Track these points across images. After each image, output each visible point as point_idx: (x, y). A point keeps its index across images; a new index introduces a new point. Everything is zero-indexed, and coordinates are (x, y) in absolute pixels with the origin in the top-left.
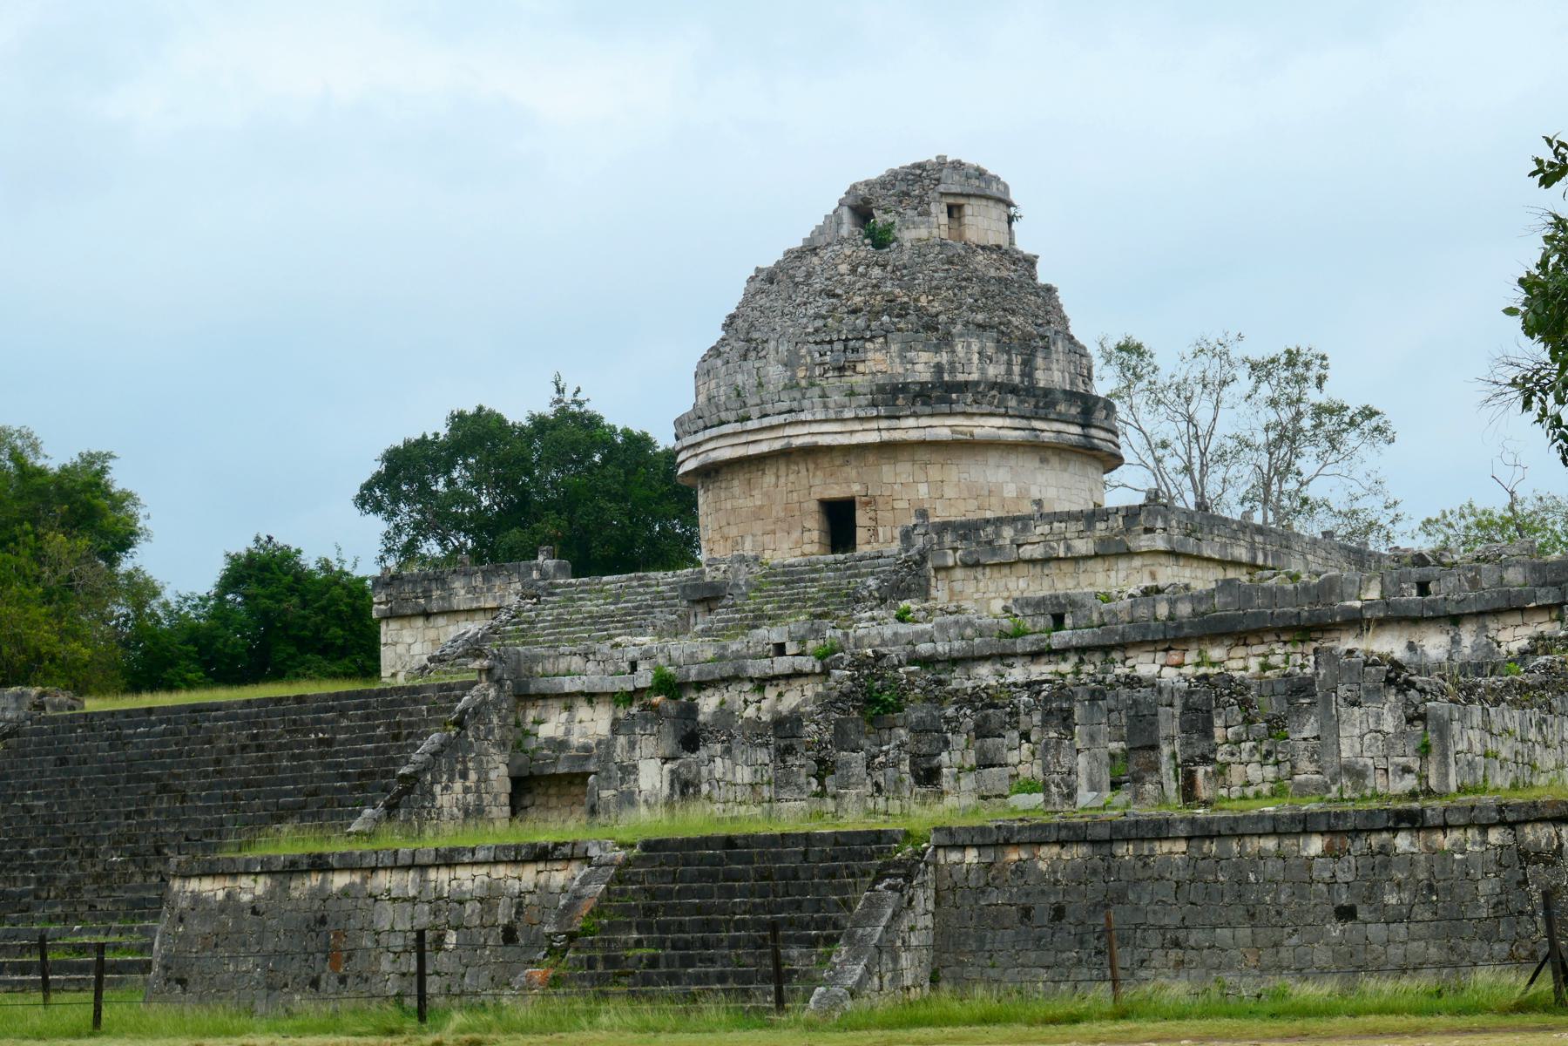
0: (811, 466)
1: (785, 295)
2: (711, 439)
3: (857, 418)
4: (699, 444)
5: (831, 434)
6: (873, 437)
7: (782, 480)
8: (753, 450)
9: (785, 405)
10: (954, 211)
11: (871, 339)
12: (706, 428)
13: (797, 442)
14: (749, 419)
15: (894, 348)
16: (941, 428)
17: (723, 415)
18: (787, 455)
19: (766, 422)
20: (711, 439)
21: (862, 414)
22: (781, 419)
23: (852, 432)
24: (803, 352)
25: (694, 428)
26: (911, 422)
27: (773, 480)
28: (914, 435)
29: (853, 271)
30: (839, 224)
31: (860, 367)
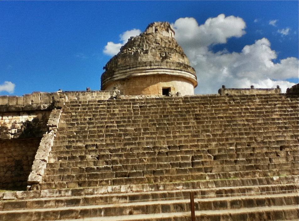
0: (160, 79)
1: (146, 42)
2: (132, 71)
3: (174, 69)
4: (126, 72)
5: (169, 72)
6: (177, 74)
7: (153, 81)
8: (147, 74)
9: (157, 64)
10: (171, 33)
11: (173, 53)
12: (130, 68)
13: (160, 73)
14: (146, 66)
15: (177, 56)
16: (187, 75)
17: (138, 65)
18: (154, 76)
19: (152, 67)
20: (132, 71)
21: (175, 68)
22: (157, 67)
23: (173, 72)
24: (158, 53)
25: (125, 68)
26: (183, 72)
27: (149, 81)
28: (184, 75)
29: (161, 39)
30: (153, 30)
31: (171, 59)
